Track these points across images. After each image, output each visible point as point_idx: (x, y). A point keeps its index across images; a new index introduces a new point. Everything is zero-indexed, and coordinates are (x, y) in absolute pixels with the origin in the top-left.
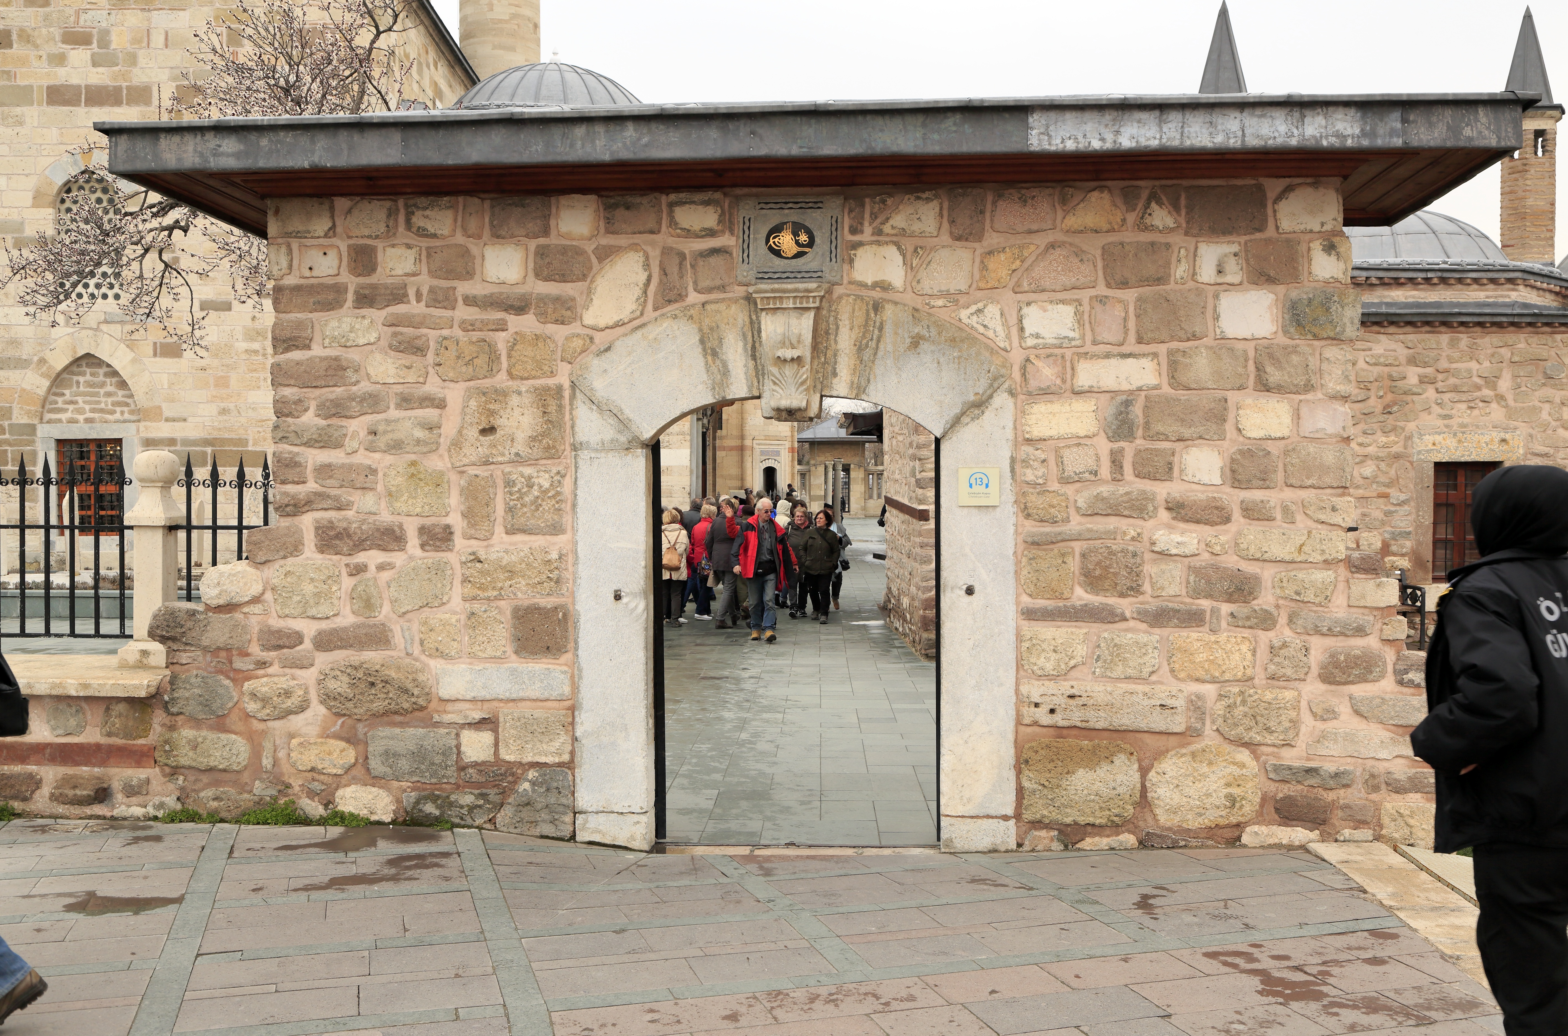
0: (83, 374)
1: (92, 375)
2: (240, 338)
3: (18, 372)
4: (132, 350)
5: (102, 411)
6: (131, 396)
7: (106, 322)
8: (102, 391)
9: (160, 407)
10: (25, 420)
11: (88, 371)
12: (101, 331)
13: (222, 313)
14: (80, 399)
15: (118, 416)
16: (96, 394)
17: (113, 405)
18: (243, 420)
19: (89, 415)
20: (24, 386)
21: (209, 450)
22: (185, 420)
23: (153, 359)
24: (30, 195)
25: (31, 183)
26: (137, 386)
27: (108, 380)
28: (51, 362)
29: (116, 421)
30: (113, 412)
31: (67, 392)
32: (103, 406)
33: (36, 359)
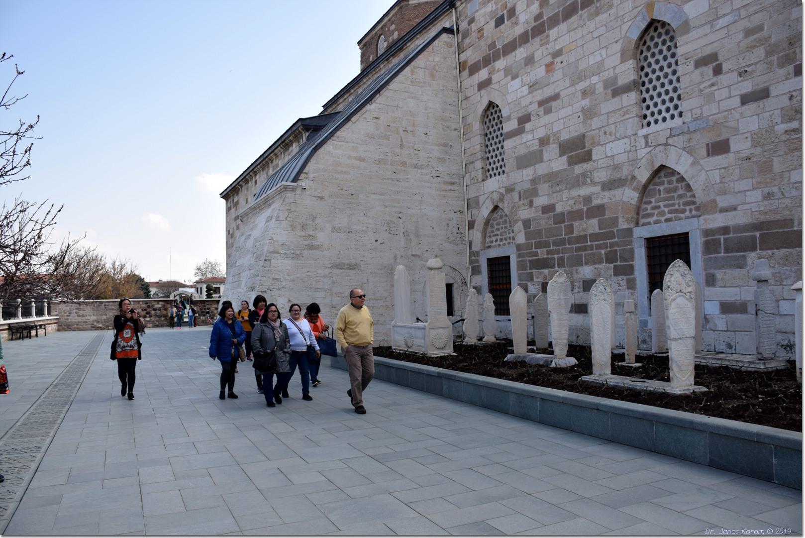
0: (662, 183)
1: (669, 182)
2: (779, 120)
3: (620, 190)
4: (691, 155)
5: (676, 211)
6: (694, 196)
7: (671, 136)
8: (676, 195)
9: (714, 201)
10: (625, 226)
11: (666, 180)
12: (669, 145)
13: (761, 103)
14: (661, 204)
15: (687, 213)
16: (672, 198)
18: (787, 201)
19: (668, 216)
20: (625, 199)
21: (758, 234)
22: (735, 209)
23: (708, 159)
24: (619, 54)
25: (617, 47)
26: (698, 186)
27: (679, 185)
28: (639, 177)
30: (684, 211)
31: (653, 200)
32: (677, 207)
33: (630, 177)
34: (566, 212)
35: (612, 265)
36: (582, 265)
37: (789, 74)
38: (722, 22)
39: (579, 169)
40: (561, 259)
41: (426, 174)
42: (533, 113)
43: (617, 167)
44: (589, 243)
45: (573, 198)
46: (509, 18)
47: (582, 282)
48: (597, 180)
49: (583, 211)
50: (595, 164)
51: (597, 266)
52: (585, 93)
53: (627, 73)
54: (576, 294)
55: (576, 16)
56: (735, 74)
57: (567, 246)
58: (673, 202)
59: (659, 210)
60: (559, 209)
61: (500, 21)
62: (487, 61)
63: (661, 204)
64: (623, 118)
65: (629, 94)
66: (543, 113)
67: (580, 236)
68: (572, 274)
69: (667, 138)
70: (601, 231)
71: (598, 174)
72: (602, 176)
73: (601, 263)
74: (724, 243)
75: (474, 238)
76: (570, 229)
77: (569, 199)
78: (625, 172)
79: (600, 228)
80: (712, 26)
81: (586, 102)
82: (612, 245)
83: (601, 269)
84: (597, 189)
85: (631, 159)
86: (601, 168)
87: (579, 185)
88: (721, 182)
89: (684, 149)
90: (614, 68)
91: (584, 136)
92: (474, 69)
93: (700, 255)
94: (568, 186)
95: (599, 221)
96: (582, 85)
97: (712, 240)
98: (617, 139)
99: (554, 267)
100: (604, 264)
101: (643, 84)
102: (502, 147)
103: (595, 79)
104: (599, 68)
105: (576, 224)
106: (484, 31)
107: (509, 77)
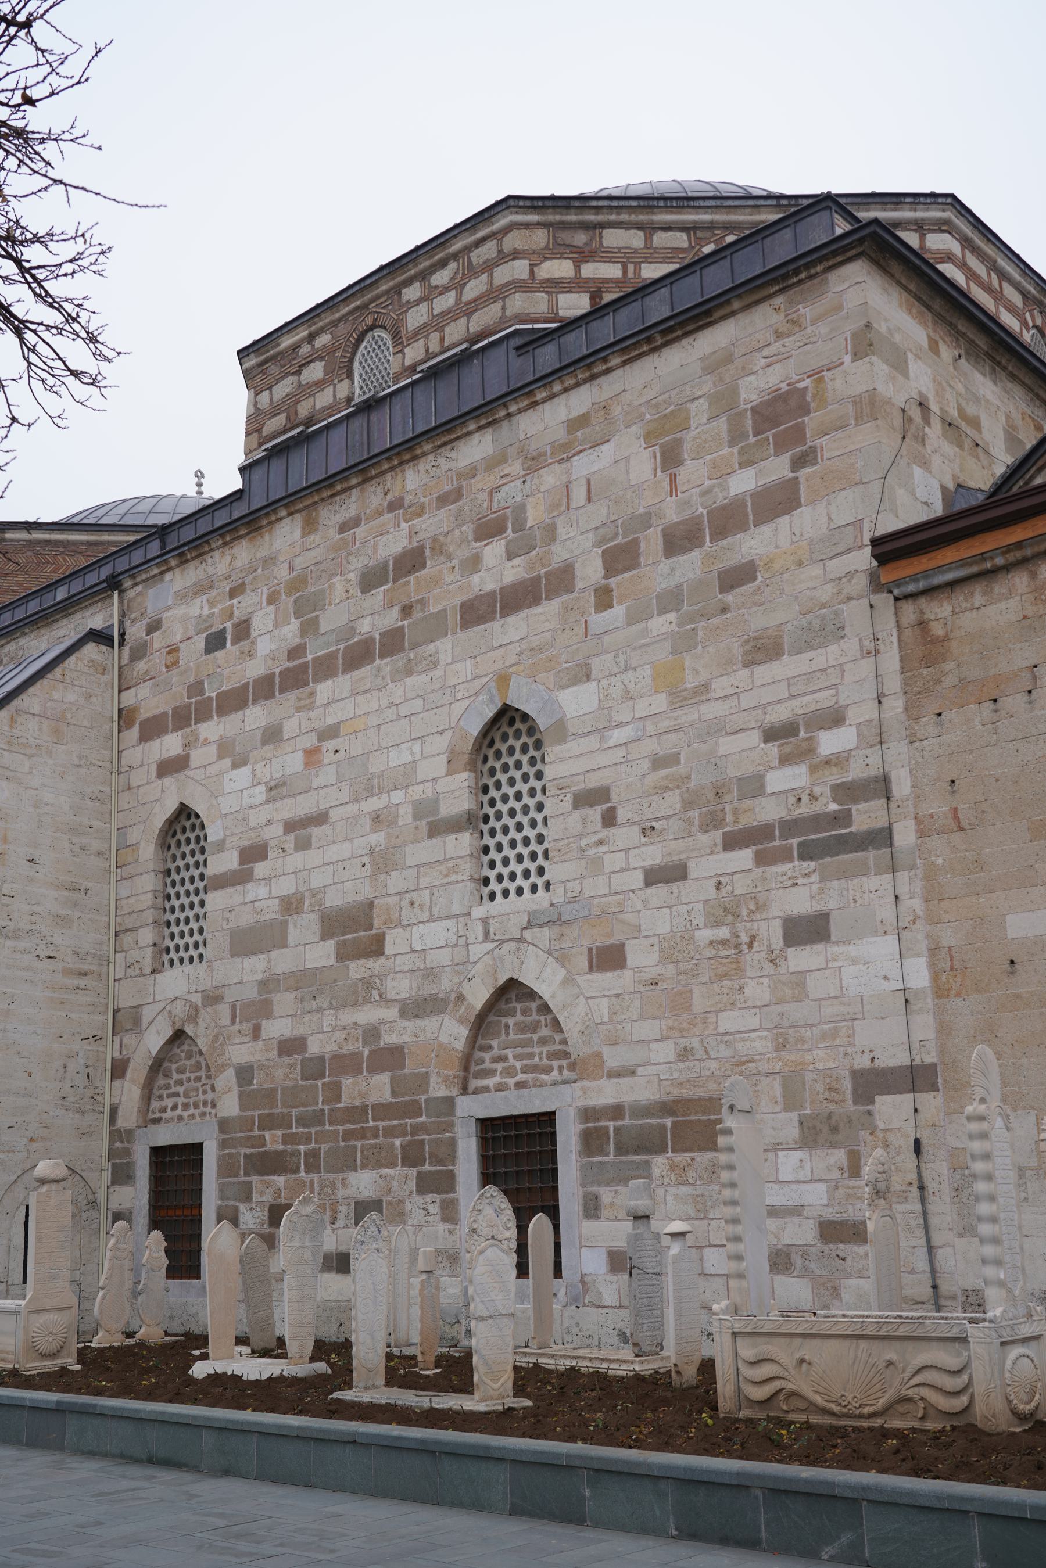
0: (512, 1013)
1: (525, 1012)
3: (434, 1019)
4: (563, 966)
5: (535, 1069)
6: (564, 1042)
7: (530, 925)
8: (535, 1037)
9: (599, 1055)
11: (518, 1006)
12: (526, 942)
13: (675, 887)
14: (509, 1053)
16: (528, 1043)
17: (548, 1058)
18: (713, 1065)
19: (521, 1077)
20: (443, 1039)
21: (668, 1122)
22: (633, 1073)
23: (589, 977)
24: (444, 758)
25: (442, 743)
26: (571, 1023)
27: (542, 1018)
29: (554, 1084)
30: (548, 1070)
31: (495, 1043)
33: (453, 996)
34: (327, 1056)
35: (413, 1172)
36: (355, 1170)
37: (715, 845)
38: (618, 736)
39: (357, 969)
40: (314, 1154)
41: (25, 951)
42: (272, 844)
43: (430, 974)
44: (371, 1123)
45: (344, 1028)
46: (236, 640)
47: (353, 1206)
48: (391, 995)
49: (363, 1056)
50: (389, 964)
51: (385, 1171)
52: (377, 819)
53: (457, 794)
54: (340, 1232)
55: (369, 667)
56: (636, 829)
57: (327, 1127)
58: (530, 1050)
59: (506, 1065)
60: (314, 1048)
61: (215, 642)
62: (182, 718)
63: (509, 1053)
64: (445, 880)
65: (459, 835)
66: (292, 846)
67: (355, 1108)
68: (334, 1188)
69: (522, 929)
70: (394, 1100)
71: (394, 984)
72: (401, 988)
73: (392, 1165)
74: (615, 1134)
75: (124, 1099)
76: (335, 1092)
77: (335, 1028)
78: (446, 984)
79: (394, 1094)
80: (602, 739)
81: (378, 838)
82: (416, 1130)
83: (393, 1178)
84: (391, 1013)
85: (456, 961)
86: (400, 972)
87: (356, 1004)
88: (611, 1021)
89: (550, 953)
90: (435, 780)
91: (371, 905)
92: (153, 729)
93: (574, 1156)
94: (334, 1002)
95: (392, 1079)
96: (373, 804)
97: (595, 1128)
98: (432, 919)
99: (296, 1171)
100: (399, 1168)
101: (486, 819)
102: (202, 904)
103: (397, 797)
104: (406, 777)
105: (347, 1082)
106: (181, 655)
107: (227, 762)
